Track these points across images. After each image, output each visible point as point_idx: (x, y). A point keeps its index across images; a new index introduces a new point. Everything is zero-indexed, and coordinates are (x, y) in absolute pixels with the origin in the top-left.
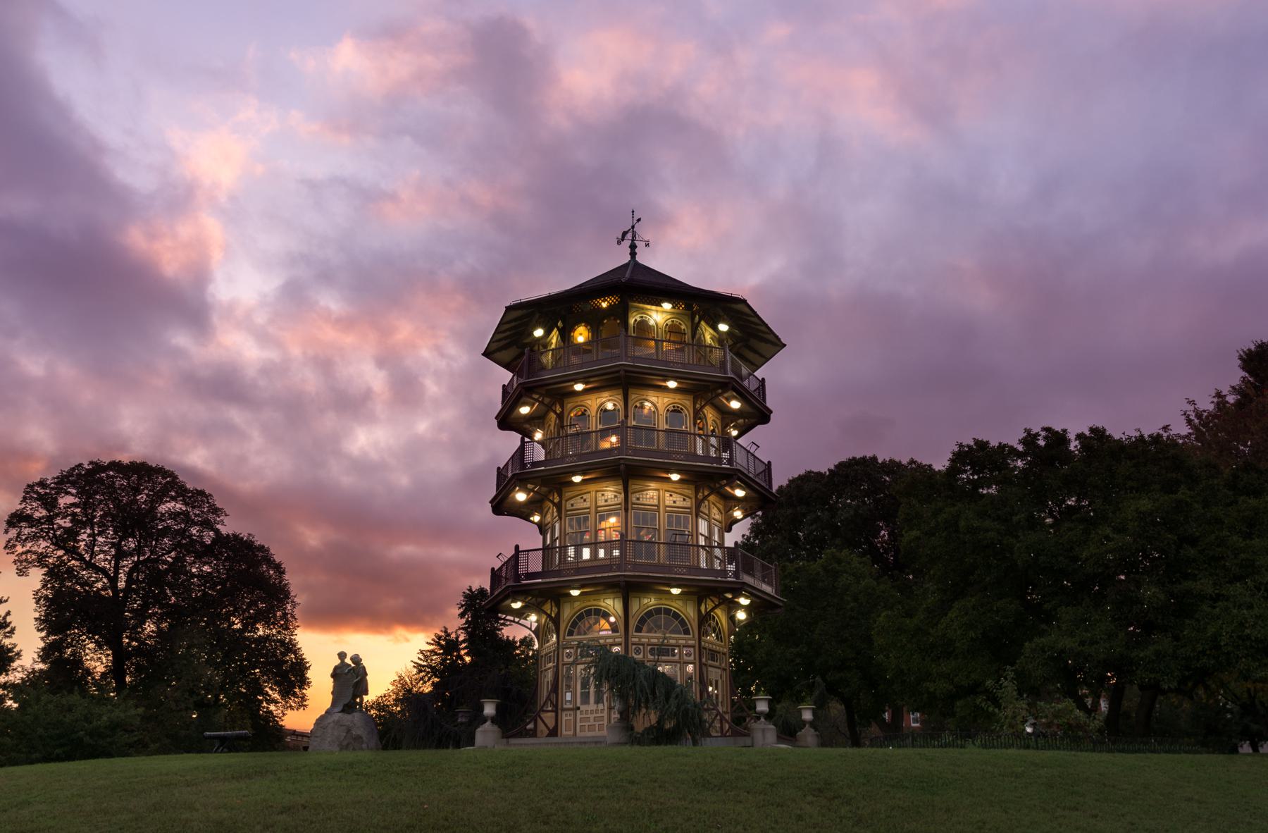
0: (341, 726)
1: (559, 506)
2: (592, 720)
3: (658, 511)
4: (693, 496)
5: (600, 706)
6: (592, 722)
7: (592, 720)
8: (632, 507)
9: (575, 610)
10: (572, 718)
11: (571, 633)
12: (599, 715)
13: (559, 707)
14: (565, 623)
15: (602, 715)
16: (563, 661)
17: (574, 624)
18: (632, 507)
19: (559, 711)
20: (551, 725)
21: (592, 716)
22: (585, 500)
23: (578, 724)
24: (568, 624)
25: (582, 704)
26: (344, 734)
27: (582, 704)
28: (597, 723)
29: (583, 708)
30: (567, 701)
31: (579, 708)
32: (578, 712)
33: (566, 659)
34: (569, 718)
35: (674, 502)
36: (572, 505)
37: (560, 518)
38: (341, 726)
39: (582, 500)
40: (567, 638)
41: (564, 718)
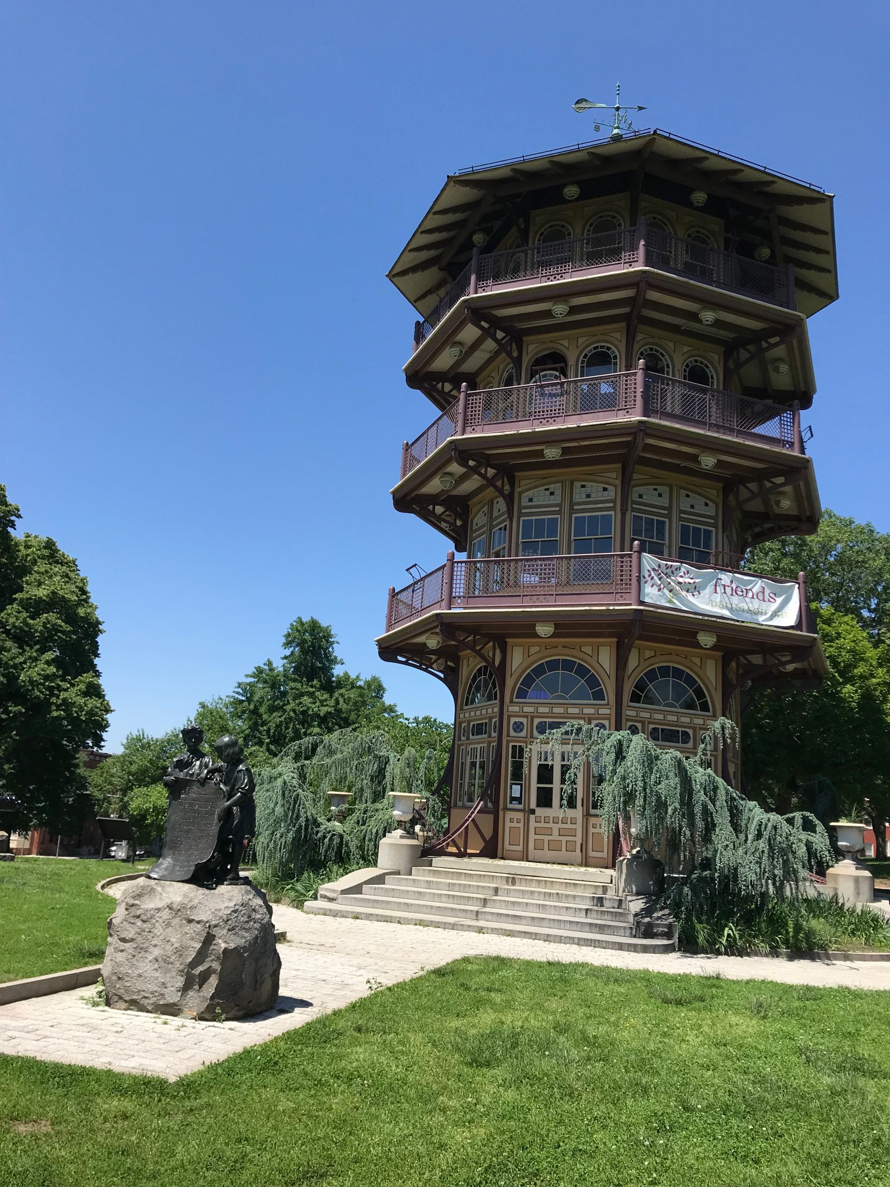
0: (190, 921)
1: (510, 499)
2: (555, 832)
3: (669, 516)
4: (720, 501)
5: (570, 813)
6: (555, 836)
7: (555, 832)
8: (632, 507)
9: (532, 659)
10: (521, 825)
11: (522, 694)
12: (569, 826)
13: (501, 807)
14: (514, 677)
15: (573, 826)
16: (508, 736)
17: (528, 681)
18: (632, 507)
19: (501, 813)
20: (488, 834)
21: (555, 828)
22: (552, 494)
23: (532, 837)
24: (520, 676)
25: (538, 805)
26: (198, 946)
27: (538, 805)
28: (564, 839)
29: (540, 812)
30: (513, 799)
31: (533, 812)
32: (532, 817)
33: (512, 733)
34: (515, 824)
35: (692, 507)
36: (531, 500)
37: (511, 519)
38: (190, 921)
39: (548, 492)
40: (515, 700)
41: (508, 825)
